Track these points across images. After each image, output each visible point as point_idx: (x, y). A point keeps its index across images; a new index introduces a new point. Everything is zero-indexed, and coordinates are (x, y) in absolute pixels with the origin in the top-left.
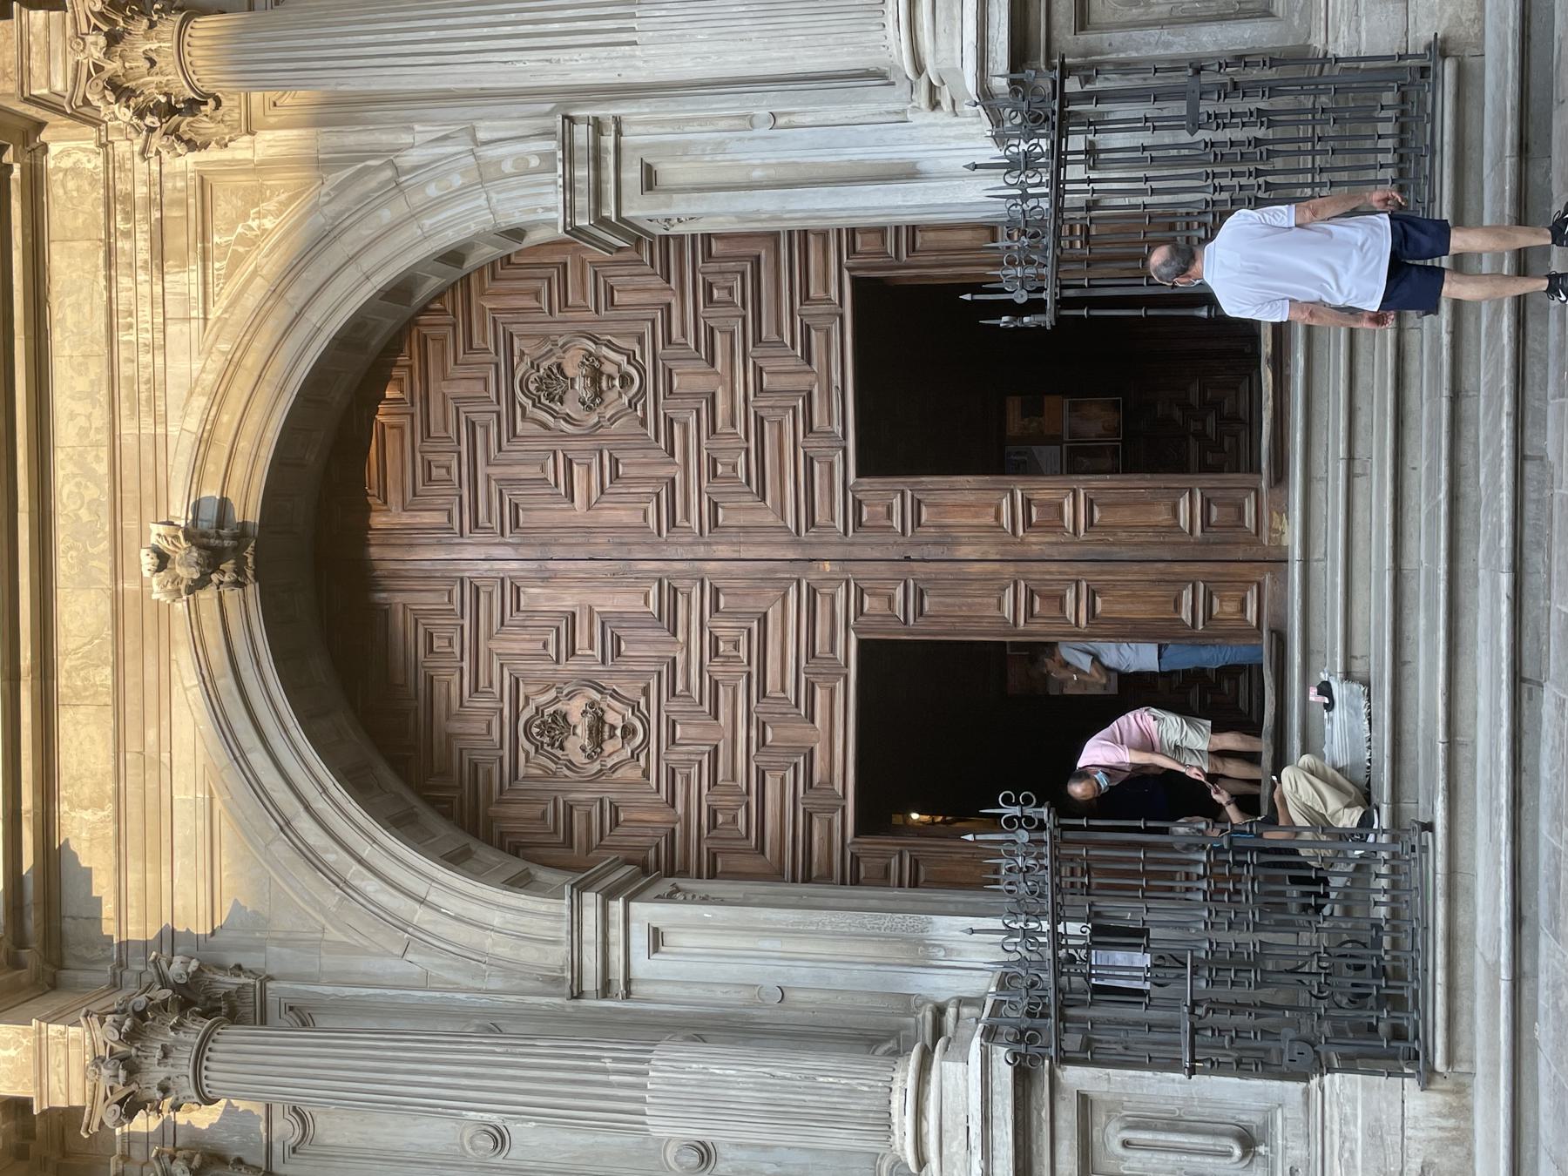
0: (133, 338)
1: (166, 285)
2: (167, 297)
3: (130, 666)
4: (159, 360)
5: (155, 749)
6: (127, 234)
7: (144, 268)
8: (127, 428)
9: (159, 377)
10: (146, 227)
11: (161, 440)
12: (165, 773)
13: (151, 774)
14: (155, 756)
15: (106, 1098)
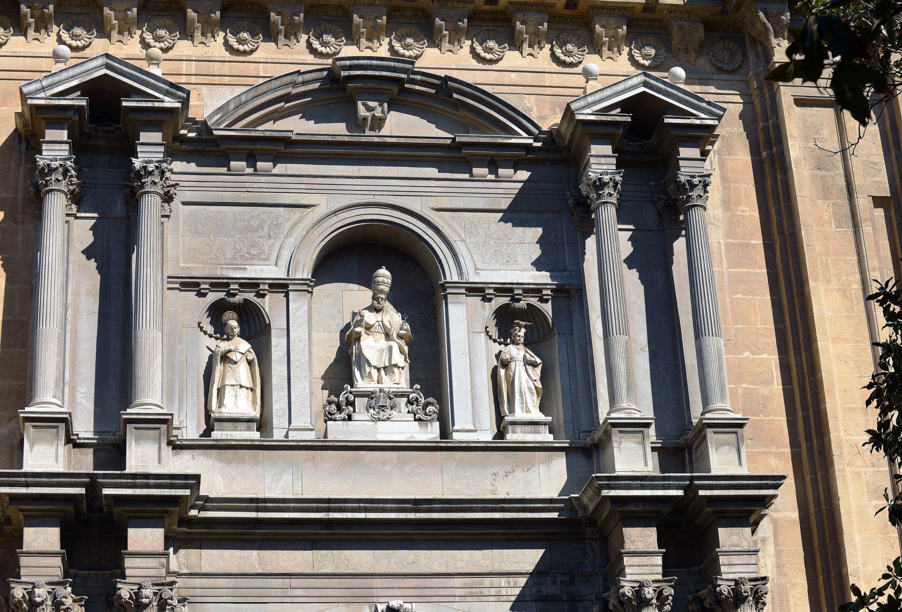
0: (503, 585)
1: (530, 603)
2: (524, 603)
3: (335, 582)
4: (493, 599)
5: (292, 594)
6: (554, 583)
7: (539, 591)
8: (457, 582)
9: (484, 599)
10: (558, 592)
11: (452, 599)
12: (279, 600)
13: (279, 592)
14: (288, 594)
15: (132, 590)
